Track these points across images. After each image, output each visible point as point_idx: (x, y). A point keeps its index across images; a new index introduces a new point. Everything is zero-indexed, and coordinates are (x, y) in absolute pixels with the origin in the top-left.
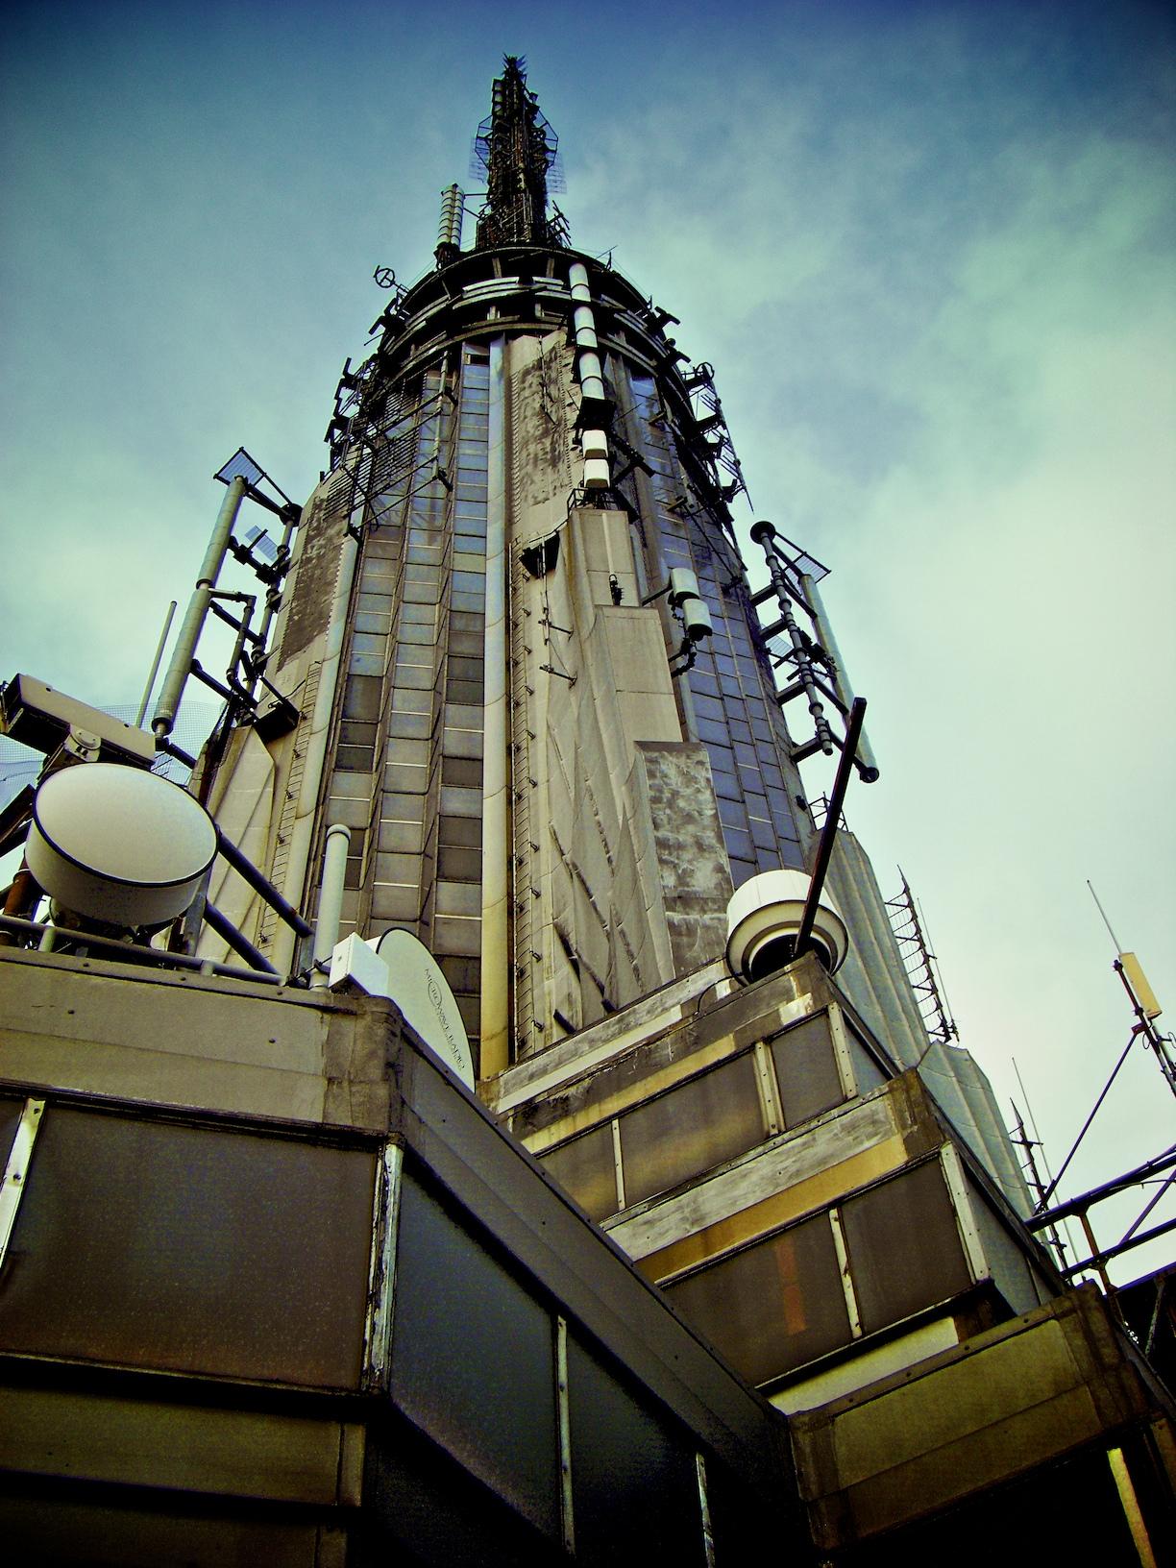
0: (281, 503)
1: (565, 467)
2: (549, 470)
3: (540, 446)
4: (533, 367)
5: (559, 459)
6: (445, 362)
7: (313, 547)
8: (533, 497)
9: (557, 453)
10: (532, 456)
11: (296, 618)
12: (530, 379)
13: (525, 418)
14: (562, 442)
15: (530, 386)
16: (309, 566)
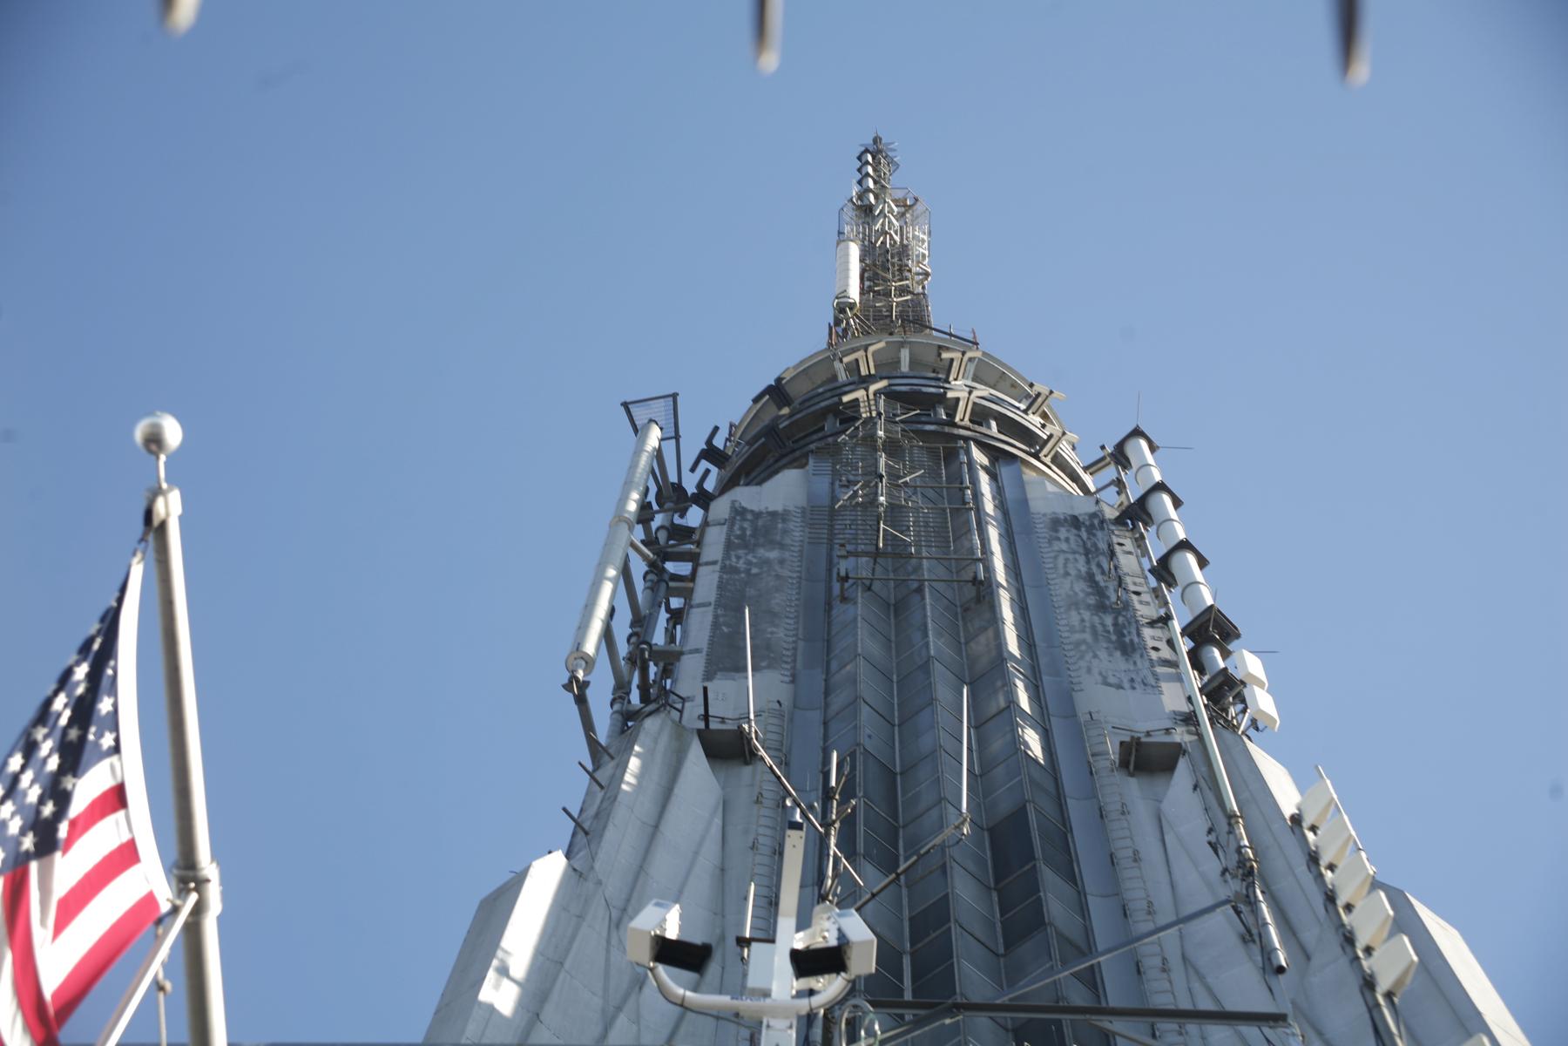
0: (673, 478)
1: (1147, 664)
2: (1118, 654)
3: (1096, 619)
4: (1066, 520)
5: (1134, 650)
6: (962, 452)
7: (738, 558)
8: (1100, 674)
9: (1127, 640)
10: (1087, 624)
11: (725, 629)
12: (1063, 533)
13: (1067, 574)
14: (1134, 632)
15: (1067, 540)
16: (737, 577)
